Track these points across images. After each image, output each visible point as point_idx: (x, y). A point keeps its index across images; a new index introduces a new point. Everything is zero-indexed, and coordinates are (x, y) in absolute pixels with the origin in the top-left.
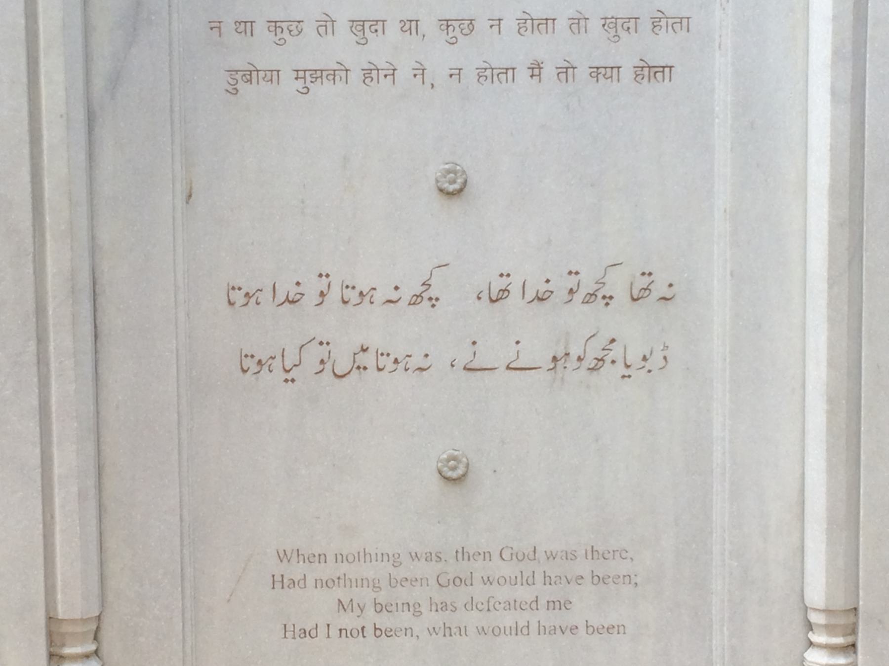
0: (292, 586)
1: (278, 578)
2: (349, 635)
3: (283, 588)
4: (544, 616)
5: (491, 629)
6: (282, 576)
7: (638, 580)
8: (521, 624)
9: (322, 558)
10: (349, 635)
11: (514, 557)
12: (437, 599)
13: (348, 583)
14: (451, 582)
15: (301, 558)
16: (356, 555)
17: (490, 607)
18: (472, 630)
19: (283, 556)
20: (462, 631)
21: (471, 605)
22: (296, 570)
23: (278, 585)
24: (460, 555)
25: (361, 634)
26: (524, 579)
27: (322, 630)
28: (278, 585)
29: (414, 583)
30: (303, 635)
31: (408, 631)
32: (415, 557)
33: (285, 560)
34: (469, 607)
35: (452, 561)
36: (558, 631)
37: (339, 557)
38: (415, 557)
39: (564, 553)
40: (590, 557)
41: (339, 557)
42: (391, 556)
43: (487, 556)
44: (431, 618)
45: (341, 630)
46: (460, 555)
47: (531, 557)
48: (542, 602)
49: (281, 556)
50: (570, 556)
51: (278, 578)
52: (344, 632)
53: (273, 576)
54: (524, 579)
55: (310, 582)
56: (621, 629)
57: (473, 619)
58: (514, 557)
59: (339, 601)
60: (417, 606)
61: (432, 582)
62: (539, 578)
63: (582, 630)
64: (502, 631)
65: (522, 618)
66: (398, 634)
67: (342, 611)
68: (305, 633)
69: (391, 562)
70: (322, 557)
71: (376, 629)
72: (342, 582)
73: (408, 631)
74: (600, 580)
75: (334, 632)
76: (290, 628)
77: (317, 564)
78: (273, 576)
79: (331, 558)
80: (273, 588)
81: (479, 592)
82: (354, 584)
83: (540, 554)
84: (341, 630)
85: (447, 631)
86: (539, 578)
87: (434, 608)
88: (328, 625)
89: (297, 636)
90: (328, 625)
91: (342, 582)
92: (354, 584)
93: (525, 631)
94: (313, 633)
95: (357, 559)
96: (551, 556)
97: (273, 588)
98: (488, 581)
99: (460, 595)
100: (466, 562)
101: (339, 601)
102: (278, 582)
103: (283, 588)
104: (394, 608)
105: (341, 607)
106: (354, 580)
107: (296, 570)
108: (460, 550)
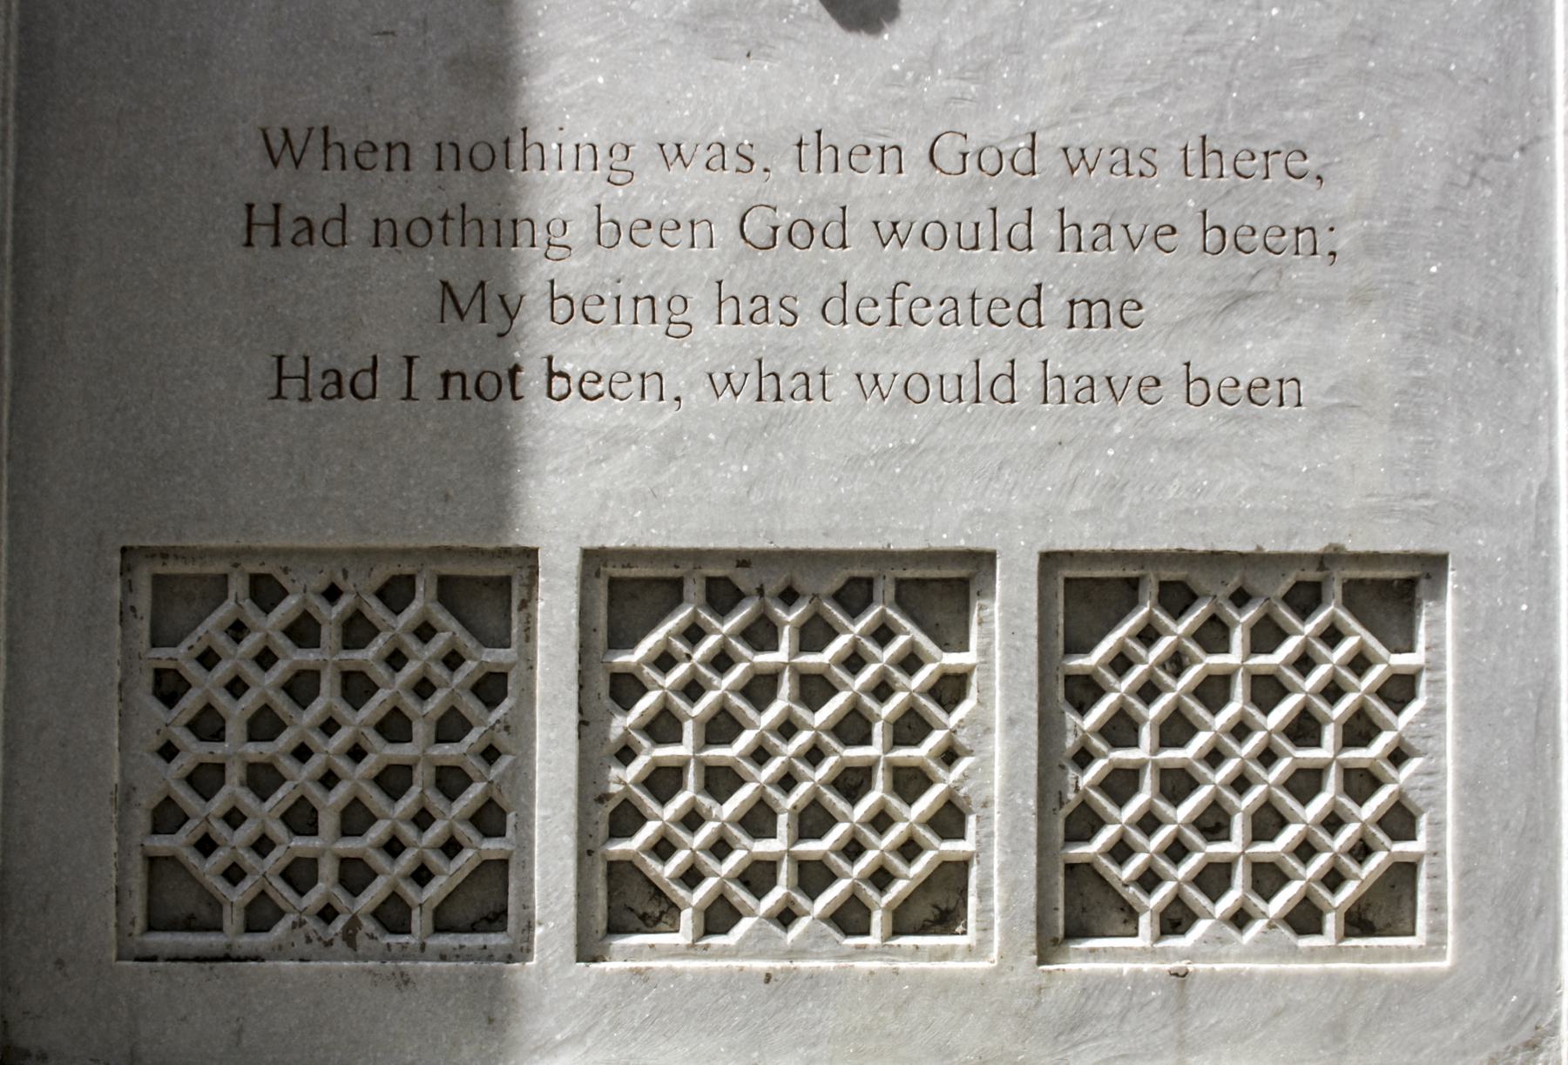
0: (304, 237)
1: (263, 214)
2: (470, 391)
3: (276, 243)
4: (1058, 347)
5: (900, 380)
6: (277, 207)
7: (1342, 244)
8: (993, 365)
9: (399, 153)
10: (470, 391)
11: (971, 163)
12: (740, 282)
13: (472, 230)
14: (781, 234)
15: (334, 155)
16: (499, 148)
17: (897, 306)
18: (842, 389)
19: (281, 149)
20: (812, 384)
21: (840, 305)
22: (318, 190)
23: (263, 235)
24: (809, 152)
25: (506, 388)
26: (1002, 234)
27: (390, 379)
28: (263, 235)
29: (667, 235)
30: (332, 391)
31: (649, 381)
32: (674, 154)
33: (286, 160)
34: (833, 311)
35: (787, 168)
36: (1101, 389)
37: (448, 152)
38: (674, 154)
39: (1120, 154)
40: (1195, 169)
41: (448, 152)
42: (602, 153)
43: (890, 156)
44: (714, 338)
45: (446, 376)
46: (809, 152)
47: (1022, 160)
48: (1054, 305)
49: (277, 144)
50: (1133, 161)
51: (263, 214)
52: (455, 382)
53: (250, 207)
54: (1002, 234)
55: (359, 229)
56: (1289, 388)
57: (848, 348)
58: (971, 163)
59: (445, 284)
60: (677, 305)
61: (725, 232)
62: (1045, 228)
63: (1172, 393)
64: (934, 389)
65: (994, 348)
66: (619, 390)
67: (452, 317)
68: (339, 383)
69: (603, 171)
70: (399, 153)
71: (551, 374)
72: (454, 227)
73: (649, 381)
74: (1225, 240)
75: (426, 379)
76: (293, 366)
77: (381, 171)
78: (250, 207)
79: (423, 156)
80: (249, 244)
81: (865, 268)
82: (490, 235)
83: (1048, 160)
84: (446, 376)
85: (769, 384)
86: (1045, 228)
87: (728, 311)
88: (410, 360)
89: (314, 391)
90: (410, 360)
91: (454, 227)
92: (490, 235)
93: (1002, 389)
94: (365, 383)
95: (500, 159)
96: (1076, 160)
97: (249, 244)
98: (891, 233)
99: (807, 272)
100: (826, 176)
101: (445, 284)
102: (265, 225)
103: (276, 243)
104: (607, 310)
105: (449, 306)
106: (489, 224)
107: (318, 190)
108: (810, 138)
